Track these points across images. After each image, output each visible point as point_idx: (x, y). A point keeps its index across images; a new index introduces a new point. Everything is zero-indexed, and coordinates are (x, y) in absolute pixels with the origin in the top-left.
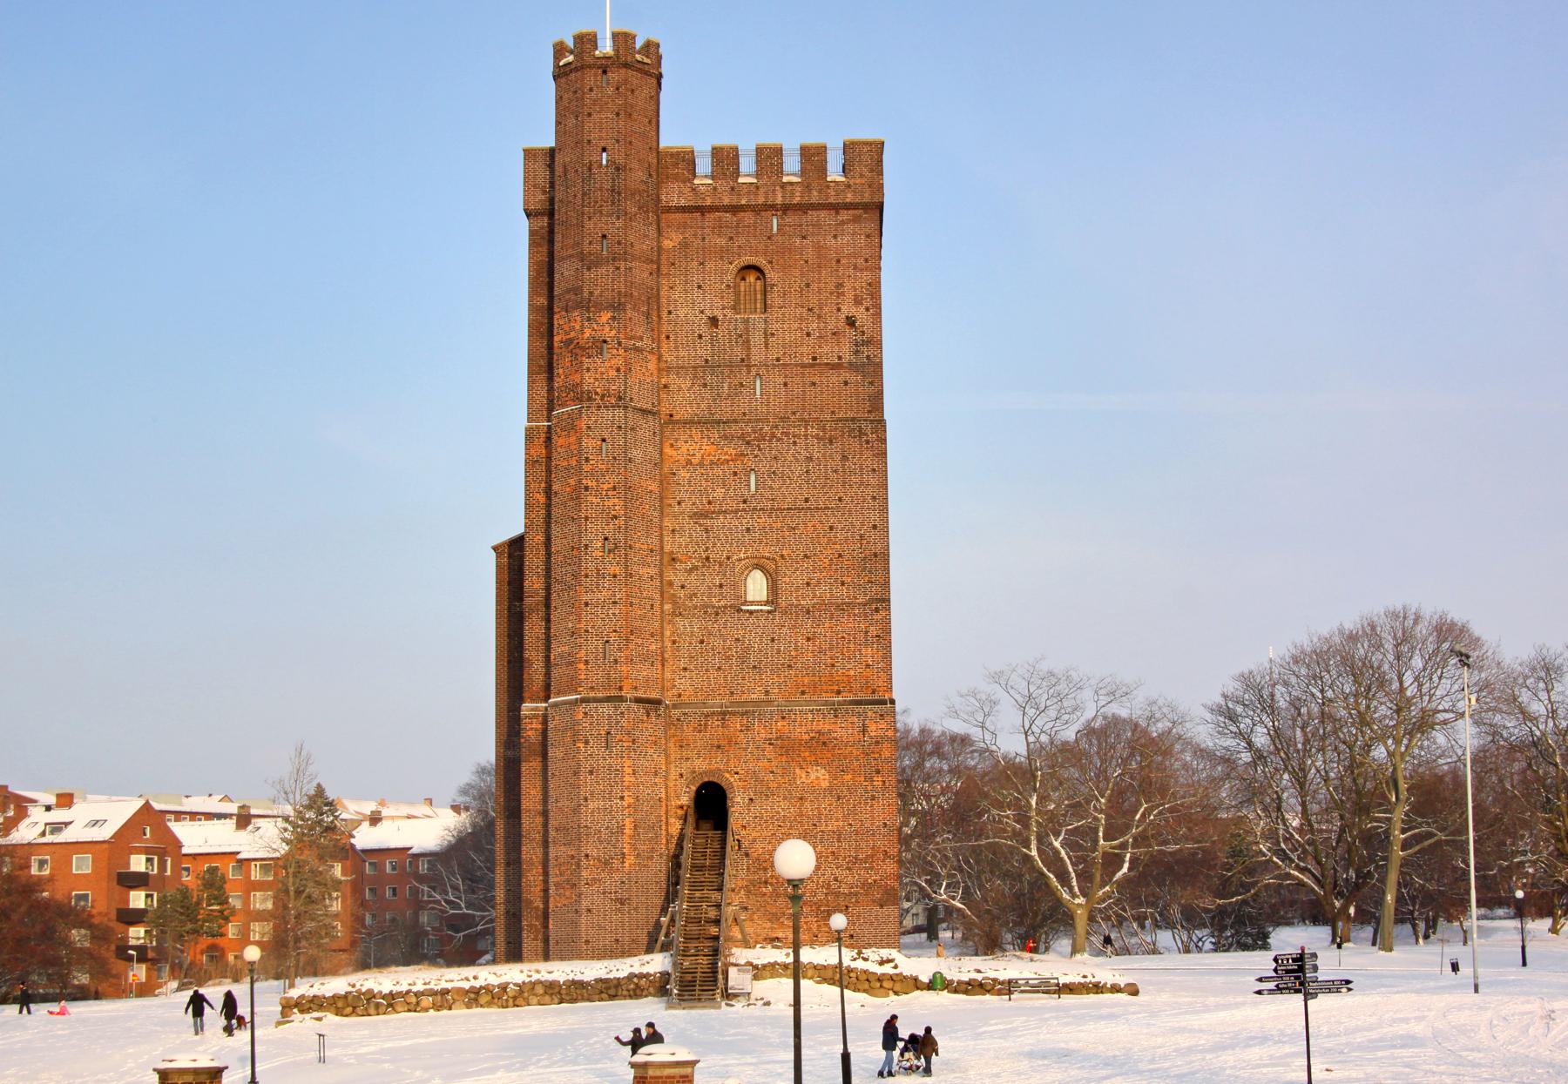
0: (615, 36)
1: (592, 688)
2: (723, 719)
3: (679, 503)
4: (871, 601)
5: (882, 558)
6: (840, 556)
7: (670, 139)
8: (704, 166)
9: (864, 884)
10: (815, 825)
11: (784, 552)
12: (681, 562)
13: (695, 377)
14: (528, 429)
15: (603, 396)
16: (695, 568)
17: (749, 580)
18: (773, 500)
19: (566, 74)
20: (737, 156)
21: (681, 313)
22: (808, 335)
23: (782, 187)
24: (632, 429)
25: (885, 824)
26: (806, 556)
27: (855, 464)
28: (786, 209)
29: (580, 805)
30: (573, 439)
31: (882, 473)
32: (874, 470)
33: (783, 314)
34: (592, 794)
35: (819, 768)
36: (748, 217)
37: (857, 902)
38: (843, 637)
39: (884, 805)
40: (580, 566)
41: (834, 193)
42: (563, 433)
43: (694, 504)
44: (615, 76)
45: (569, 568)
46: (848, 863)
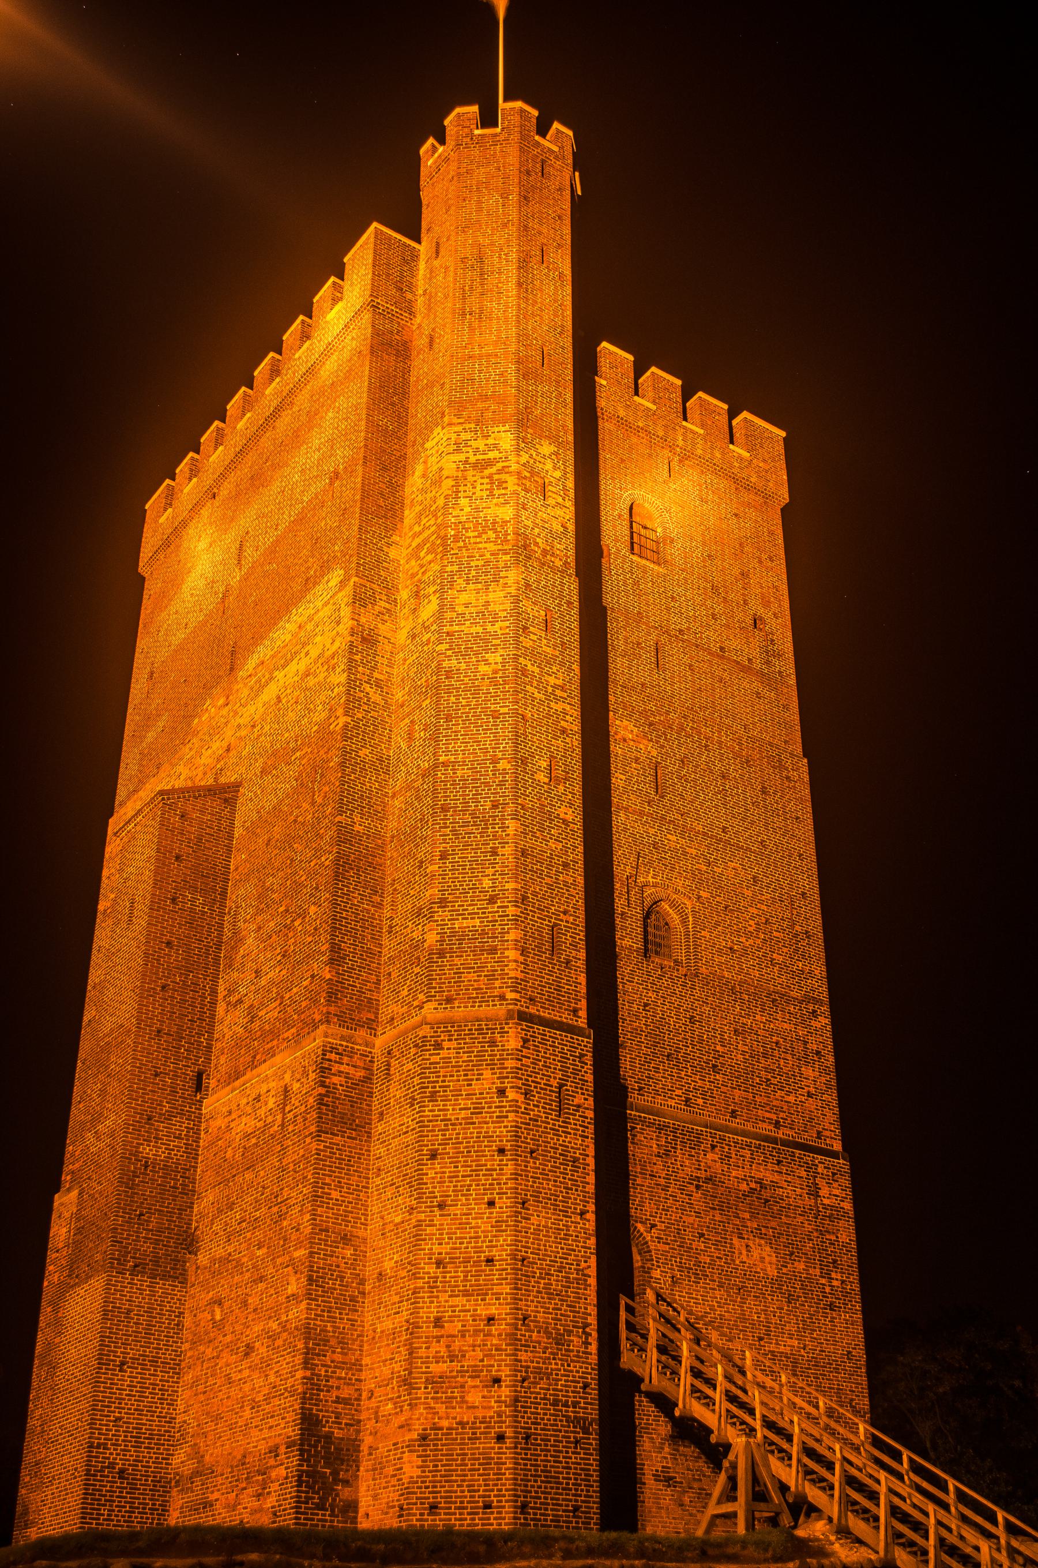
6: (767, 920)
10: (761, 1339)
32: (797, 818)
33: (685, 579)
35: (763, 1242)
42: (472, 586)
45: (484, 791)
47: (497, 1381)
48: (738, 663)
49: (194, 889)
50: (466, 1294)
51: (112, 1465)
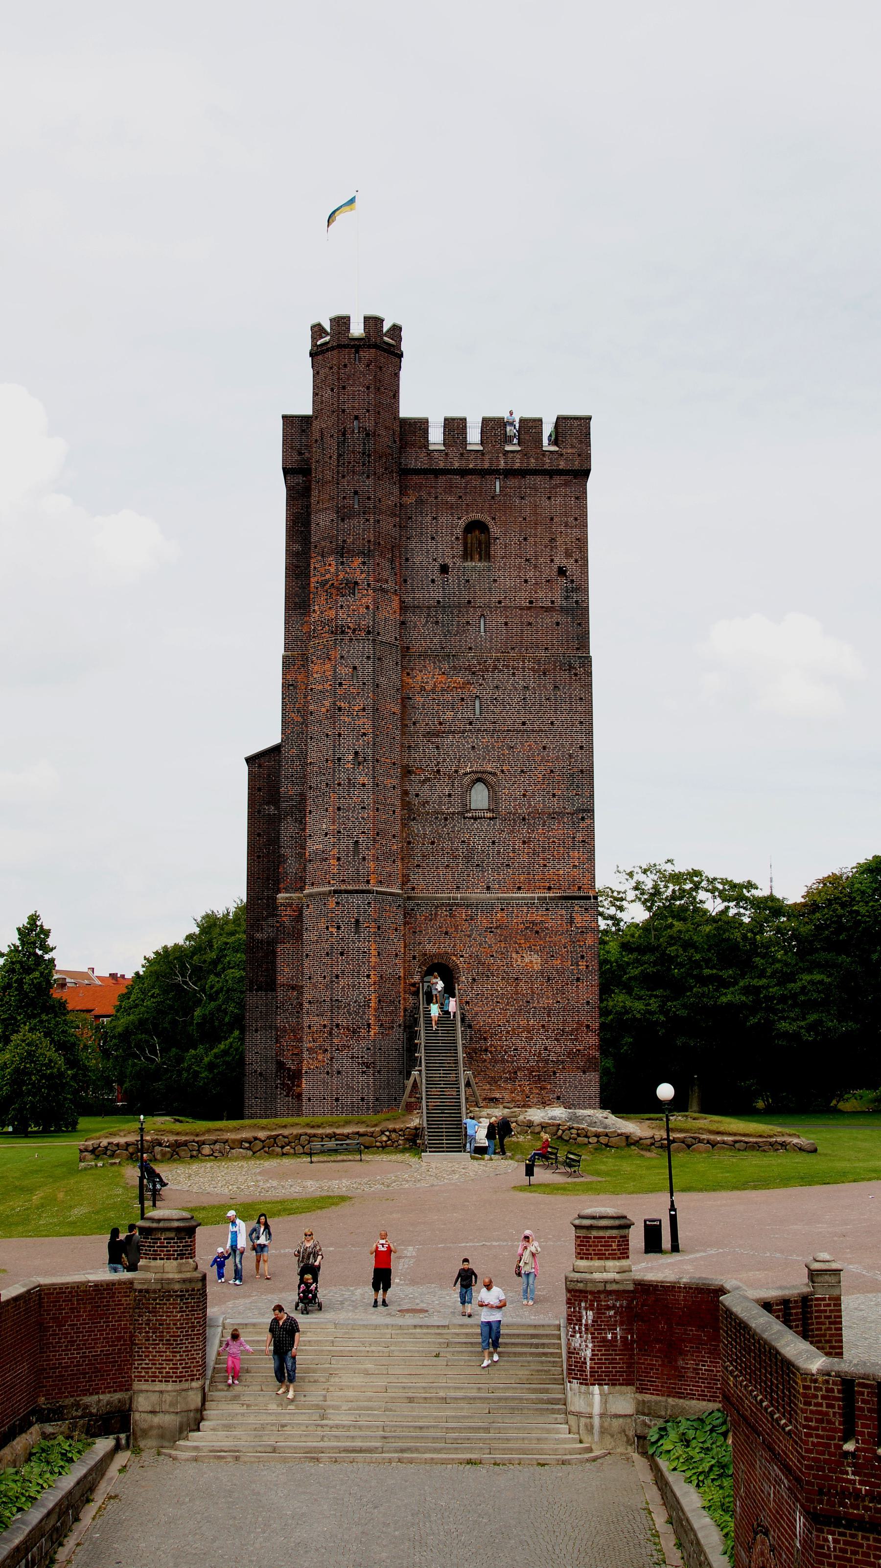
0: (367, 319)
1: (343, 881)
2: (451, 910)
3: (414, 723)
4: (579, 811)
5: (588, 773)
6: (552, 771)
7: (408, 409)
8: (436, 436)
9: (569, 1054)
10: (528, 1002)
11: (504, 768)
12: (416, 774)
13: (429, 615)
14: (284, 657)
15: (354, 630)
16: (427, 780)
17: (473, 791)
18: (494, 723)
19: (323, 352)
20: (465, 427)
21: (417, 560)
22: (526, 581)
23: (504, 455)
24: (379, 659)
25: (588, 1003)
26: (522, 771)
27: (565, 693)
28: (509, 473)
29: (332, 982)
30: (328, 666)
31: (586, 700)
32: (581, 699)
33: (505, 564)
34: (343, 972)
36: (475, 481)
37: (564, 1068)
38: (554, 842)
39: (587, 986)
40: (334, 775)
41: (548, 461)
43: (427, 724)
44: (365, 354)
45: (323, 778)
46: (556, 1035)
47: (326, 1050)
48: (543, 607)
49: (268, 804)
50: (318, 1016)
51: (256, 1071)
